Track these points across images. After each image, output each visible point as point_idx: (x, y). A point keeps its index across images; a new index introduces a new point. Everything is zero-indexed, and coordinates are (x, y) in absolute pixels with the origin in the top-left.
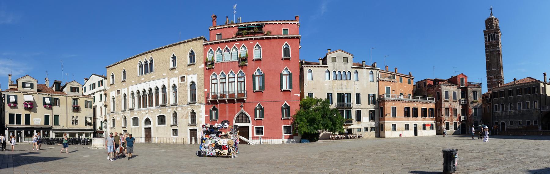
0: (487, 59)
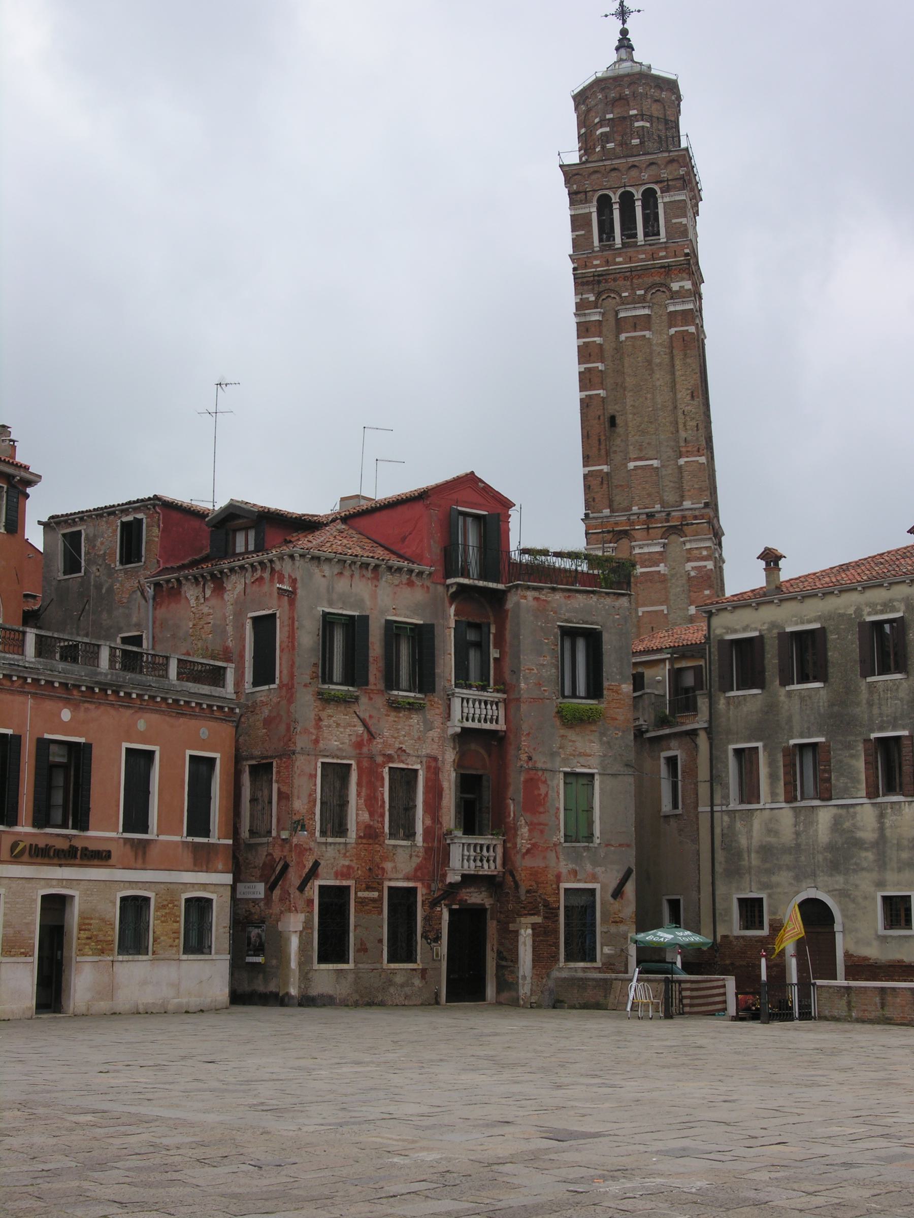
0: (586, 380)
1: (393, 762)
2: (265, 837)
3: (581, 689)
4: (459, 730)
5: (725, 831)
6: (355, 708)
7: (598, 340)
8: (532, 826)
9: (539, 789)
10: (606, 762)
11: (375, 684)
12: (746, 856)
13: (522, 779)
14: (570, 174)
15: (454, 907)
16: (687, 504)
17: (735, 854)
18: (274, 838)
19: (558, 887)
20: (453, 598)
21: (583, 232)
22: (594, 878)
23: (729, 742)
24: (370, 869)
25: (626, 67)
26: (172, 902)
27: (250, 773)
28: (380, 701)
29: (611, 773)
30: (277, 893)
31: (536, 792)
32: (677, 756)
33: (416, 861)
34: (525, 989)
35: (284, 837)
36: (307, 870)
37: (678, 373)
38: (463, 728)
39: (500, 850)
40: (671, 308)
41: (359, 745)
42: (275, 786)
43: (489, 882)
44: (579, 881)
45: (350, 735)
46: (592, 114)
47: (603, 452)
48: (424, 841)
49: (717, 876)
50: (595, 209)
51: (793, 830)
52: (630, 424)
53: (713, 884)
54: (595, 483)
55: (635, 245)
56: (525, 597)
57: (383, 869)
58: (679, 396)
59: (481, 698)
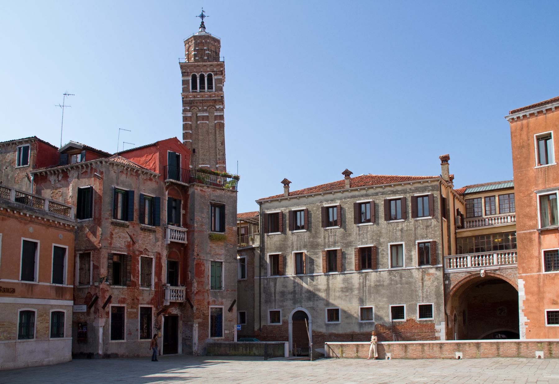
1: (142, 254)
2: (86, 285)
3: (218, 228)
4: (169, 242)
5: (265, 286)
6: (127, 230)
7: (190, 123)
8: (199, 283)
9: (201, 267)
10: (227, 257)
11: (136, 221)
12: (273, 295)
13: (195, 263)
14: (183, 66)
15: (167, 315)
17: (269, 295)
18: (91, 285)
19: (208, 307)
20: (167, 188)
21: (186, 86)
22: (222, 304)
23: (268, 252)
24: (133, 299)
25: (203, 33)
26: (45, 313)
27: (80, 257)
28: (138, 229)
29: (228, 261)
30: (93, 309)
31: (200, 269)
32: (245, 258)
33: (152, 296)
35: (96, 285)
36: (106, 300)
37: (217, 136)
38: (171, 242)
39: (184, 292)
40: (216, 114)
41: (128, 246)
42: (92, 263)
43: (181, 305)
44: (216, 305)
45: (125, 242)
46: (191, 47)
48: (155, 288)
49: (262, 303)
50: (190, 78)
51: (293, 285)
53: (260, 306)
55: (204, 92)
56: (197, 189)
57: (138, 299)
58: (217, 144)
59: (178, 229)
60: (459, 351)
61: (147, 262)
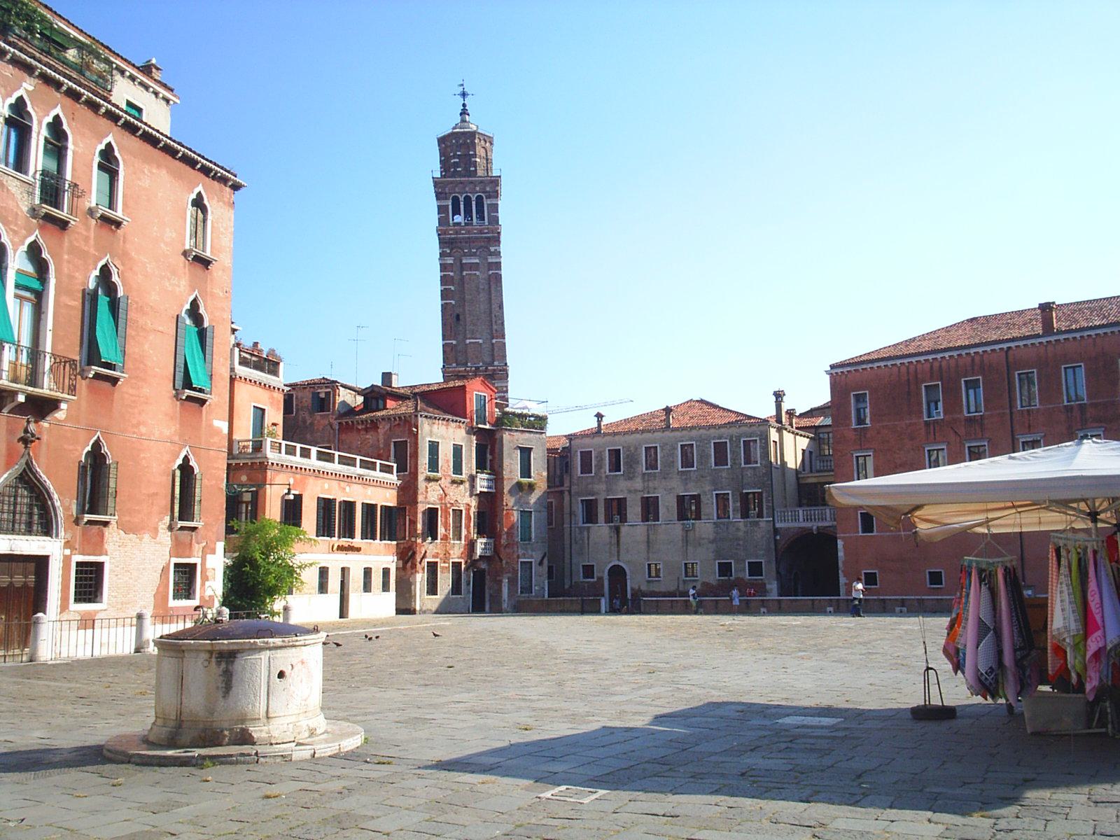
0: (445, 295)
7: (451, 274)
14: (436, 183)
16: (496, 363)
22: (532, 557)
23: (579, 496)
33: (462, 550)
34: (505, 606)
40: (490, 260)
41: (441, 499)
47: (453, 334)
50: (450, 203)
52: (468, 320)
54: (448, 349)
58: (493, 306)
60: (764, 607)
61: (458, 513)
